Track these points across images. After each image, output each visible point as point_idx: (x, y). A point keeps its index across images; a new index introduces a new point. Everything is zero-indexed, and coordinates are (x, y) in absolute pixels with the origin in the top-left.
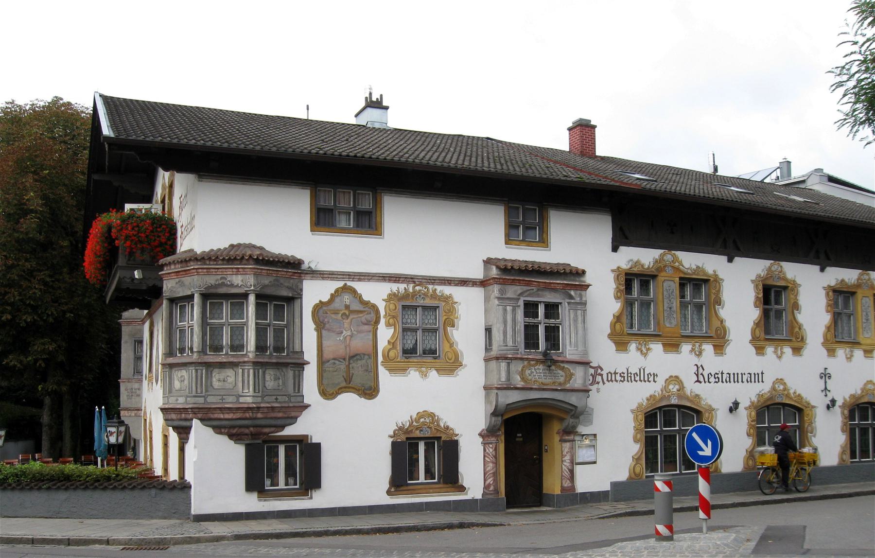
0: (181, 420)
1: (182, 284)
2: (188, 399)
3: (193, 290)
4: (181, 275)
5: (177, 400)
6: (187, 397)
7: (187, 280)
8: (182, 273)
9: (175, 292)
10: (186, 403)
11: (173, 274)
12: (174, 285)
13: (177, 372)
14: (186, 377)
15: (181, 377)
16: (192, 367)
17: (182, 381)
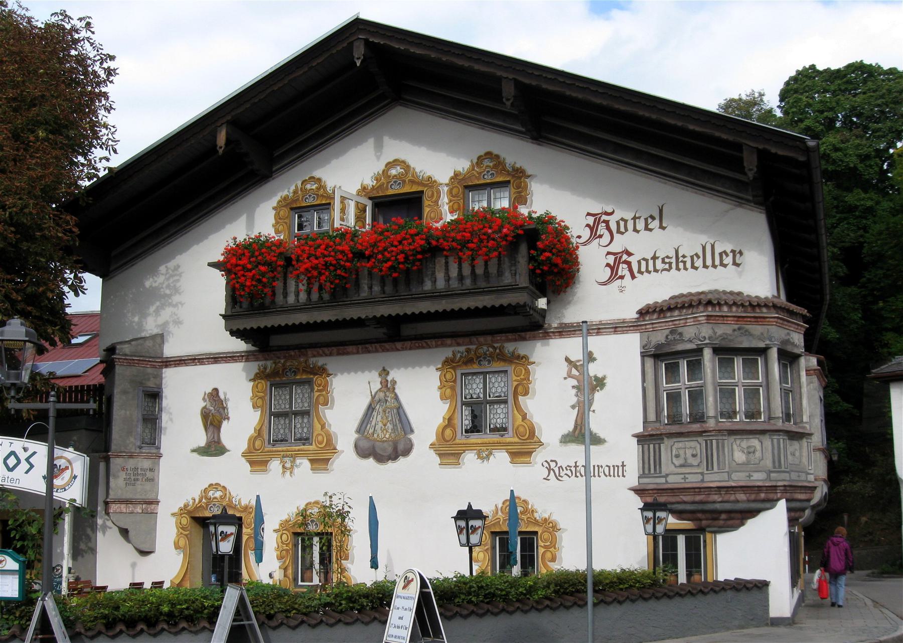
0: (748, 501)
1: (747, 333)
2: (772, 475)
3: (768, 342)
4: (747, 321)
5: (750, 476)
6: (771, 472)
7: (757, 329)
8: (749, 319)
9: (730, 341)
10: (769, 478)
11: (729, 319)
12: (729, 332)
13: (738, 442)
14: (758, 447)
15: (748, 447)
16: (779, 435)
17: (750, 453)
